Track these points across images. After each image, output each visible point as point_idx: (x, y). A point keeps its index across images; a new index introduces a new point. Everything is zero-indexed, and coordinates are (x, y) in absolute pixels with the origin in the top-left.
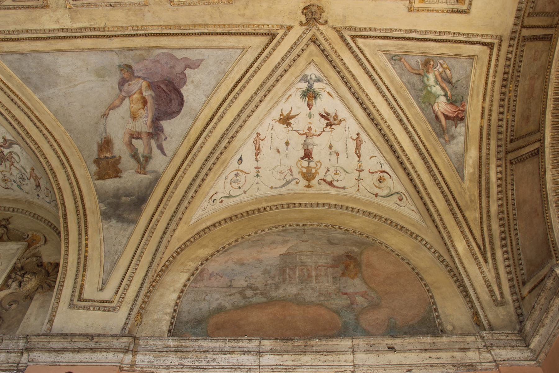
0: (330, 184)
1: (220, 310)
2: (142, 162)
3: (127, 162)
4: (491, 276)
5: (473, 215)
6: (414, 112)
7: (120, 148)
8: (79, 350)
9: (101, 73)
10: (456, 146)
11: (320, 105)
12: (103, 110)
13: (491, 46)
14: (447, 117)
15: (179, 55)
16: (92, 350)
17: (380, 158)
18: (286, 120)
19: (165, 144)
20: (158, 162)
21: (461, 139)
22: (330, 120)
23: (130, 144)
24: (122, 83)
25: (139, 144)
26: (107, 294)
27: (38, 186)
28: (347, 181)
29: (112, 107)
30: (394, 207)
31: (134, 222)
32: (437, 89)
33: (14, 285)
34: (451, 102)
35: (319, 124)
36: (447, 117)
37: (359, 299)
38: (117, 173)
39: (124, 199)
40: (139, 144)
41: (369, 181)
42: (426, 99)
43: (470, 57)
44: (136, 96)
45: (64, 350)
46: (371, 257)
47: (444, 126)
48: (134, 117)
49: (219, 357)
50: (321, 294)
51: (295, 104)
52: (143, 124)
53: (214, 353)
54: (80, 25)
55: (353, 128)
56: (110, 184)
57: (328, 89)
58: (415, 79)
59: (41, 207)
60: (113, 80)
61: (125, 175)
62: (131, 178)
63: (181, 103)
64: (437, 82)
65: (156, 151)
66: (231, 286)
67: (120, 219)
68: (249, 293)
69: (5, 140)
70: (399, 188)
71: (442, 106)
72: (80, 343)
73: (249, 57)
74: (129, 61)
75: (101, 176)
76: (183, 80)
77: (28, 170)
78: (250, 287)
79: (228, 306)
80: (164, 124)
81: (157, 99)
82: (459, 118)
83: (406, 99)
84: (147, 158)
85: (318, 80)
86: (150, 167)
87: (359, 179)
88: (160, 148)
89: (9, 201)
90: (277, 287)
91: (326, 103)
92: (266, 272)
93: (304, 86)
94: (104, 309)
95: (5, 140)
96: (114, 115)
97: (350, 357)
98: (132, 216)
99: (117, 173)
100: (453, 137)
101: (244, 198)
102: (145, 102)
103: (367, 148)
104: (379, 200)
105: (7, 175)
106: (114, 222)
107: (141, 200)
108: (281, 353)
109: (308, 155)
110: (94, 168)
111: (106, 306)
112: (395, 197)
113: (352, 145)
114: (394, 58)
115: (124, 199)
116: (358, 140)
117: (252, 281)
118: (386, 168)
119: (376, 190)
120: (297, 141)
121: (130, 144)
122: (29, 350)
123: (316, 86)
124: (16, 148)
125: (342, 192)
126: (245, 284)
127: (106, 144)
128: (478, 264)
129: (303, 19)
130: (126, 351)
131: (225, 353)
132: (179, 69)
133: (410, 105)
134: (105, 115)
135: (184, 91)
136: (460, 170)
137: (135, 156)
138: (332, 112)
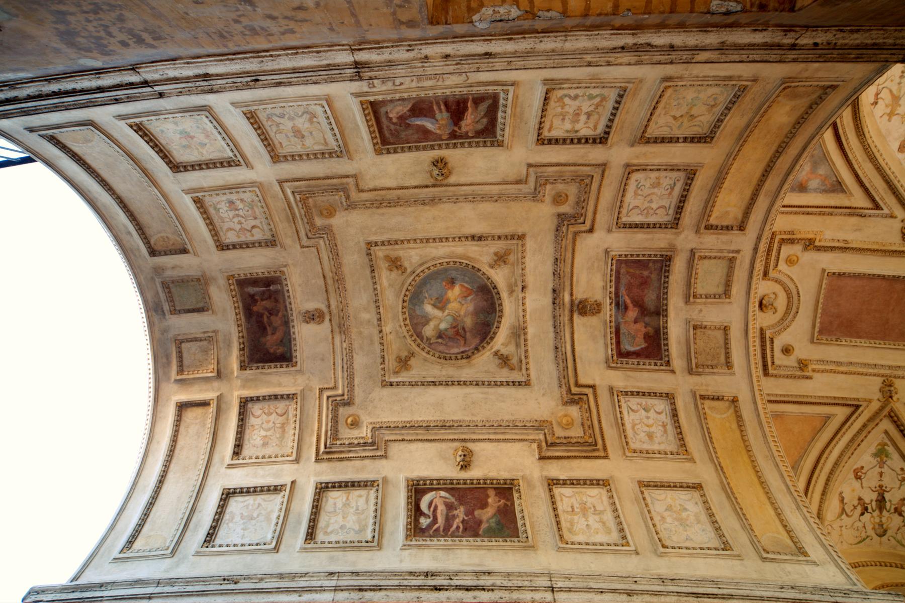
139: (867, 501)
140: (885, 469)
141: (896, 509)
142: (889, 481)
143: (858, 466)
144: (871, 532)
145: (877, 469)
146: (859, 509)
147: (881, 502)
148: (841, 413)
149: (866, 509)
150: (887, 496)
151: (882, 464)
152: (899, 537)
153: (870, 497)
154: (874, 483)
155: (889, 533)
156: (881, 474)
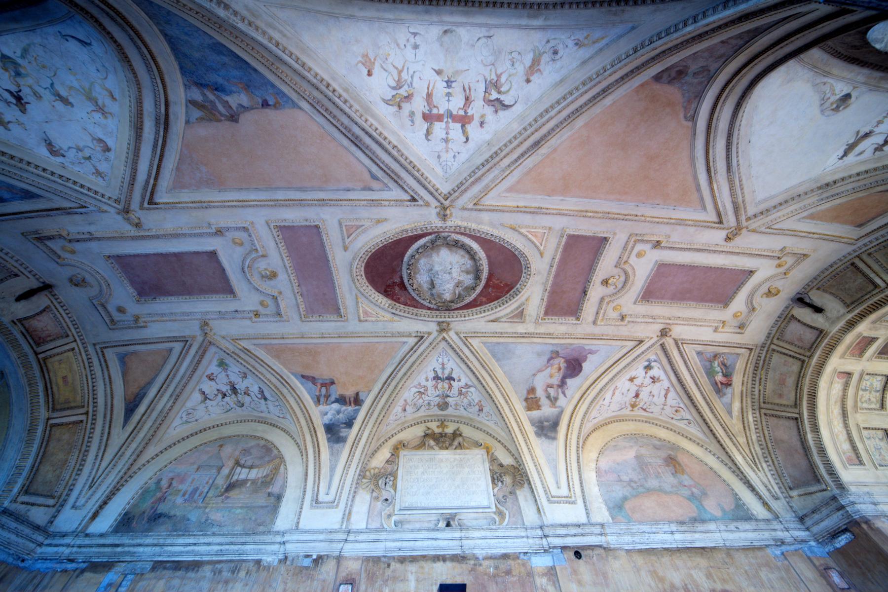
0: (645, 410)
1: (625, 499)
2: (553, 401)
3: (544, 401)
4: (765, 480)
5: (742, 440)
6: (704, 380)
7: (540, 393)
8: (575, 535)
9: (539, 354)
10: (726, 399)
11: (651, 373)
12: (534, 372)
13: (751, 350)
14: (722, 383)
15: (587, 348)
16: (582, 535)
17: (679, 400)
18: (631, 380)
19: (567, 392)
20: (562, 401)
21: (729, 395)
22: (654, 380)
23: (546, 390)
24: (549, 360)
25: (552, 391)
26: (564, 491)
27: (481, 410)
28: (656, 410)
29: (540, 371)
30: (684, 426)
31: (554, 438)
32: (718, 369)
33: (500, 484)
34: (725, 376)
35: (648, 381)
36: (722, 383)
37: (694, 490)
38: (538, 407)
39: (546, 424)
40: (552, 391)
41: (668, 411)
42: (710, 373)
43: (739, 354)
44: (557, 366)
45: (566, 536)
46: (682, 459)
47: (721, 387)
48: (551, 376)
49: (652, 535)
50: (672, 487)
51: (638, 371)
52: (556, 381)
53: (649, 533)
54: (539, 331)
55: (666, 384)
56: (535, 414)
57: (659, 365)
58: (708, 363)
59: (480, 422)
60: (545, 358)
61: (543, 408)
62: (547, 410)
63: (580, 371)
64: (719, 365)
65: (561, 396)
66: (621, 481)
67: (546, 436)
68: (633, 484)
69: (467, 385)
70: (689, 417)
71: (719, 378)
72: (573, 531)
73: (625, 351)
74: (559, 349)
75: (529, 409)
76: (585, 360)
77: (476, 401)
78: (631, 481)
79: (627, 494)
80: (569, 381)
81: (567, 368)
82: (728, 385)
83: (701, 374)
84: (556, 399)
85: (655, 361)
86: (558, 403)
87: (663, 409)
88: (564, 393)
89: (455, 416)
90: (646, 481)
91: (656, 372)
92: (634, 470)
93: (647, 363)
94: (569, 502)
95: (467, 385)
96: (540, 376)
97: (719, 534)
98: (553, 435)
99: (538, 407)
100: (725, 394)
101: (601, 418)
102: (560, 369)
103: (672, 394)
104: (673, 422)
105: (459, 402)
106: (543, 439)
107: (555, 425)
108: (684, 532)
109: (637, 396)
110: (524, 404)
111: (568, 500)
112: (686, 422)
113: (663, 393)
114: (699, 354)
115: (546, 424)
116: (667, 391)
117: (630, 476)
118: (682, 405)
119: (672, 416)
120: (634, 389)
121: (546, 390)
122: (546, 536)
123: (653, 364)
124: (472, 389)
125: (650, 415)
126: (628, 479)
127: (532, 390)
128: (754, 471)
129: (659, 334)
130: (601, 535)
131: (655, 533)
132: (584, 354)
133: (702, 377)
134: (534, 375)
135: (584, 365)
136: (730, 413)
137: (548, 397)
138: (656, 375)
139: (224, 390)
140: (229, 373)
141: (245, 393)
142: (234, 378)
143: (208, 372)
144: (233, 405)
145: (223, 374)
146: (220, 396)
147: (234, 390)
148: (177, 347)
149: (225, 395)
150: (237, 386)
151: (226, 370)
152: (252, 406)
153: (225, 388)
154: (225, 380)
155: (246, 405)
156: (228, 376)
